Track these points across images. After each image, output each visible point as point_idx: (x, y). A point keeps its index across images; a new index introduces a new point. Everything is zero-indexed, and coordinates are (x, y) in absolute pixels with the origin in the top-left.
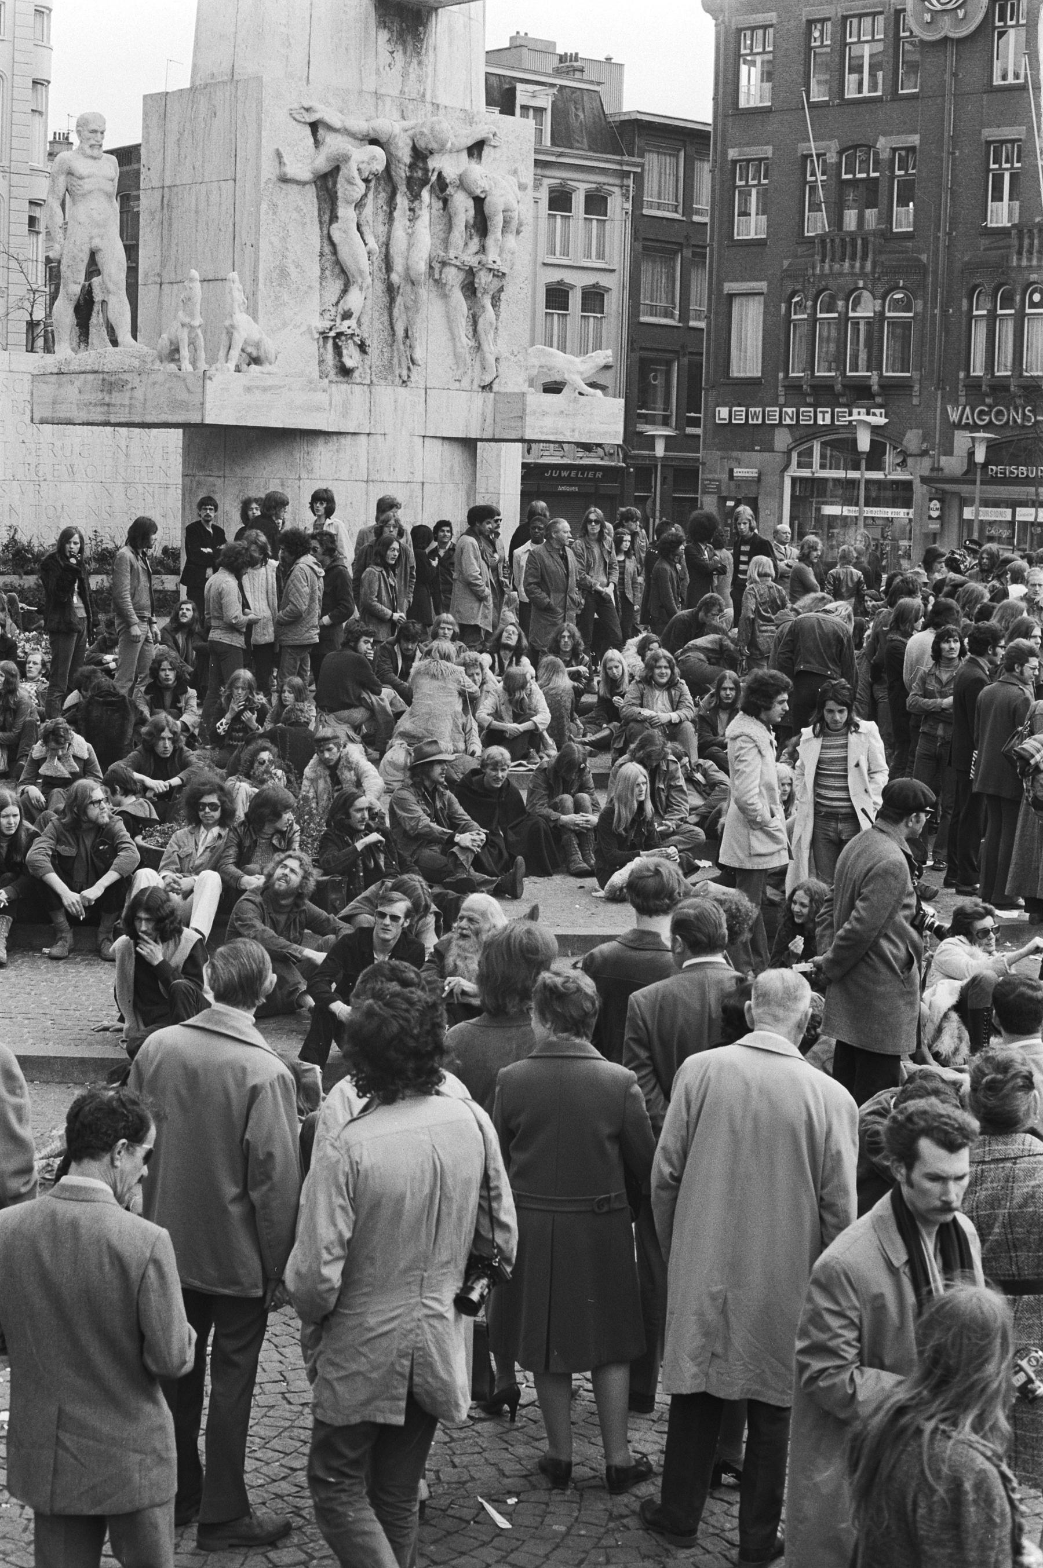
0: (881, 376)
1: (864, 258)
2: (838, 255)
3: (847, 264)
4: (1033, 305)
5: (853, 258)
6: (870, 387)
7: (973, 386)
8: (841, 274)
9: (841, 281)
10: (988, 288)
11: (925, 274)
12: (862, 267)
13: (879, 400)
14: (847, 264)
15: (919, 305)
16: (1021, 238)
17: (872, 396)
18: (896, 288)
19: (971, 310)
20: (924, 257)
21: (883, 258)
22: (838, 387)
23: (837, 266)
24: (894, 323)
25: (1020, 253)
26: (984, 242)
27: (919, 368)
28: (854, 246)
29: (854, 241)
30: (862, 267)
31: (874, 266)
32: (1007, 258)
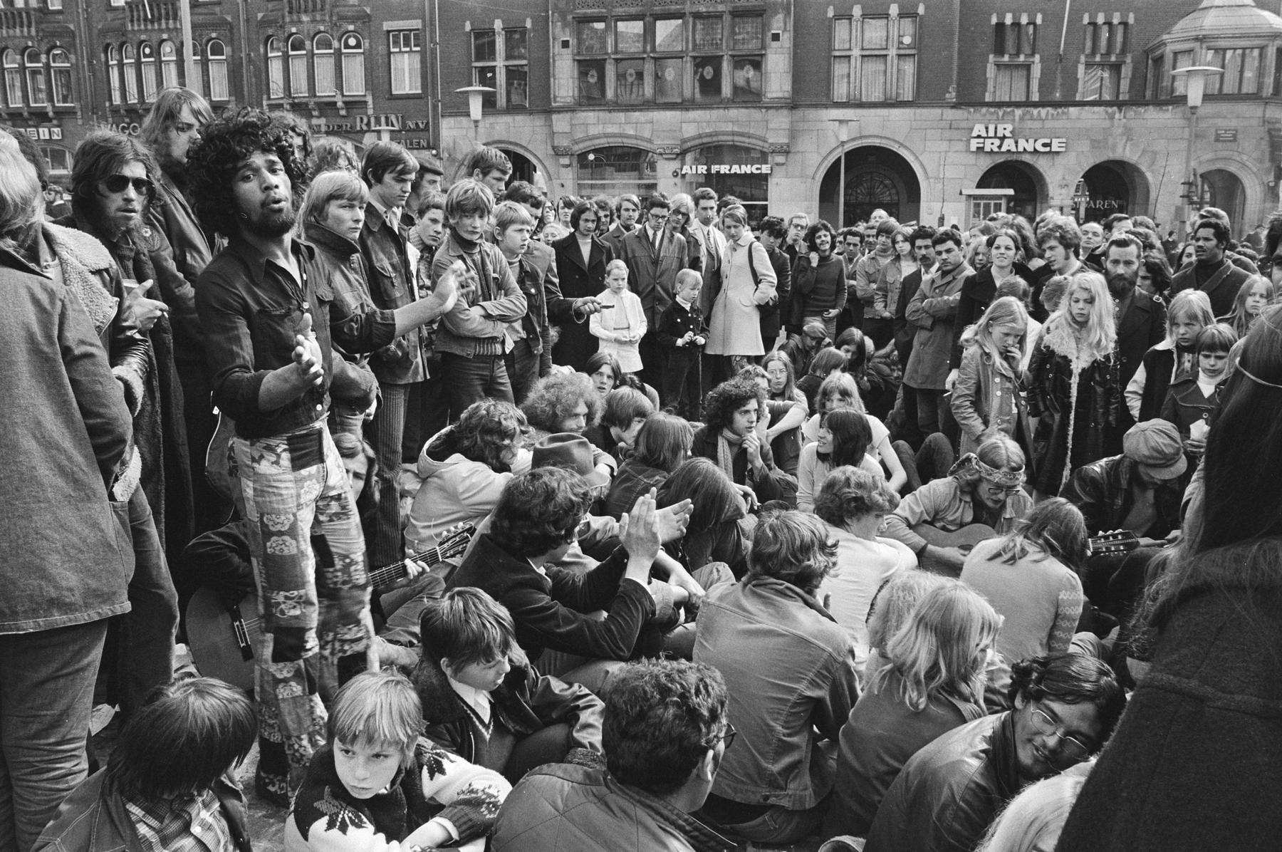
0: (54, 106)
1: (29, 26)
2: (11, 22)
3: (18, 30)
4: (145, 56)
5: (22, 26)
6: (47, 114)
7: (115, 111)
8: (15, 37)
9: (16, 41)
10: (115, 45)
11: (74, 37)
12: (29, 32)
13: (55, 122)
14: (18, 30)
15: (72, 57)
16: (132, 11)
17: (50, 120)
18: (55, 47)
19: (107, 61)
20: (72, 26)
21: (43, 26)
22: (26, 114)
23: (11, 32)
24: (60, 71)
25: (132, 21)
26: (110, 16)
27: (79, 99)
28: (21, 17)
29: (20, 14)
30: (29, 32)
31: (37, 32)
32: (124, 25)
